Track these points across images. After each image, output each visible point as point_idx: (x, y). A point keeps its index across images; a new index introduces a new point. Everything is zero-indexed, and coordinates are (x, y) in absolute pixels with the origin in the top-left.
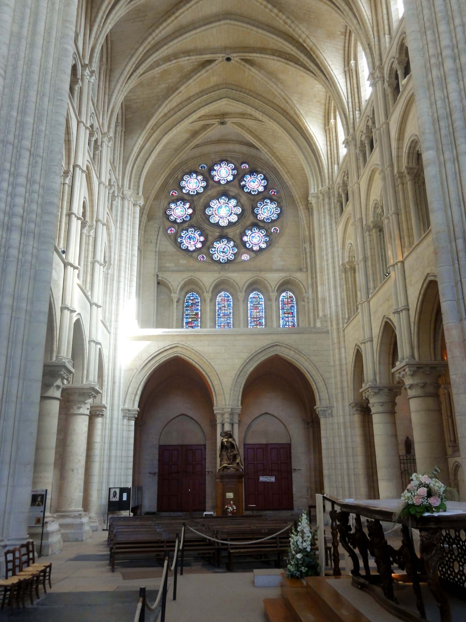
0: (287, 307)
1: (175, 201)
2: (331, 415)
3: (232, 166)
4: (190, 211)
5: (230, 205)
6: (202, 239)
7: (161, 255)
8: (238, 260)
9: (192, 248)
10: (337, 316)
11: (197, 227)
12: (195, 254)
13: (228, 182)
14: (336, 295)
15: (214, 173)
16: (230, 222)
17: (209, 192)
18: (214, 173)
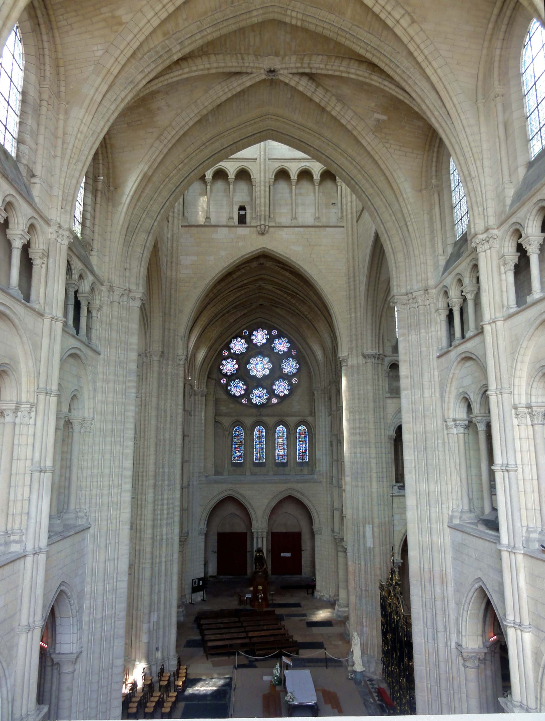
0: (302, 437)
1: (226, 358)
2: (321, 534)
3: (266, 331)
4: (237, 366)
5: (264, 362)
6: (245, 387)
7: (217, 401)
8: (269, 404)
9: (238, 394)
10: (326, 473)
12: (239, 399)
13: (263, 344)
14: (326, 460)
15: (253, 337)
16: (264, 375)
17: (250, 353)
18: (253, 337)
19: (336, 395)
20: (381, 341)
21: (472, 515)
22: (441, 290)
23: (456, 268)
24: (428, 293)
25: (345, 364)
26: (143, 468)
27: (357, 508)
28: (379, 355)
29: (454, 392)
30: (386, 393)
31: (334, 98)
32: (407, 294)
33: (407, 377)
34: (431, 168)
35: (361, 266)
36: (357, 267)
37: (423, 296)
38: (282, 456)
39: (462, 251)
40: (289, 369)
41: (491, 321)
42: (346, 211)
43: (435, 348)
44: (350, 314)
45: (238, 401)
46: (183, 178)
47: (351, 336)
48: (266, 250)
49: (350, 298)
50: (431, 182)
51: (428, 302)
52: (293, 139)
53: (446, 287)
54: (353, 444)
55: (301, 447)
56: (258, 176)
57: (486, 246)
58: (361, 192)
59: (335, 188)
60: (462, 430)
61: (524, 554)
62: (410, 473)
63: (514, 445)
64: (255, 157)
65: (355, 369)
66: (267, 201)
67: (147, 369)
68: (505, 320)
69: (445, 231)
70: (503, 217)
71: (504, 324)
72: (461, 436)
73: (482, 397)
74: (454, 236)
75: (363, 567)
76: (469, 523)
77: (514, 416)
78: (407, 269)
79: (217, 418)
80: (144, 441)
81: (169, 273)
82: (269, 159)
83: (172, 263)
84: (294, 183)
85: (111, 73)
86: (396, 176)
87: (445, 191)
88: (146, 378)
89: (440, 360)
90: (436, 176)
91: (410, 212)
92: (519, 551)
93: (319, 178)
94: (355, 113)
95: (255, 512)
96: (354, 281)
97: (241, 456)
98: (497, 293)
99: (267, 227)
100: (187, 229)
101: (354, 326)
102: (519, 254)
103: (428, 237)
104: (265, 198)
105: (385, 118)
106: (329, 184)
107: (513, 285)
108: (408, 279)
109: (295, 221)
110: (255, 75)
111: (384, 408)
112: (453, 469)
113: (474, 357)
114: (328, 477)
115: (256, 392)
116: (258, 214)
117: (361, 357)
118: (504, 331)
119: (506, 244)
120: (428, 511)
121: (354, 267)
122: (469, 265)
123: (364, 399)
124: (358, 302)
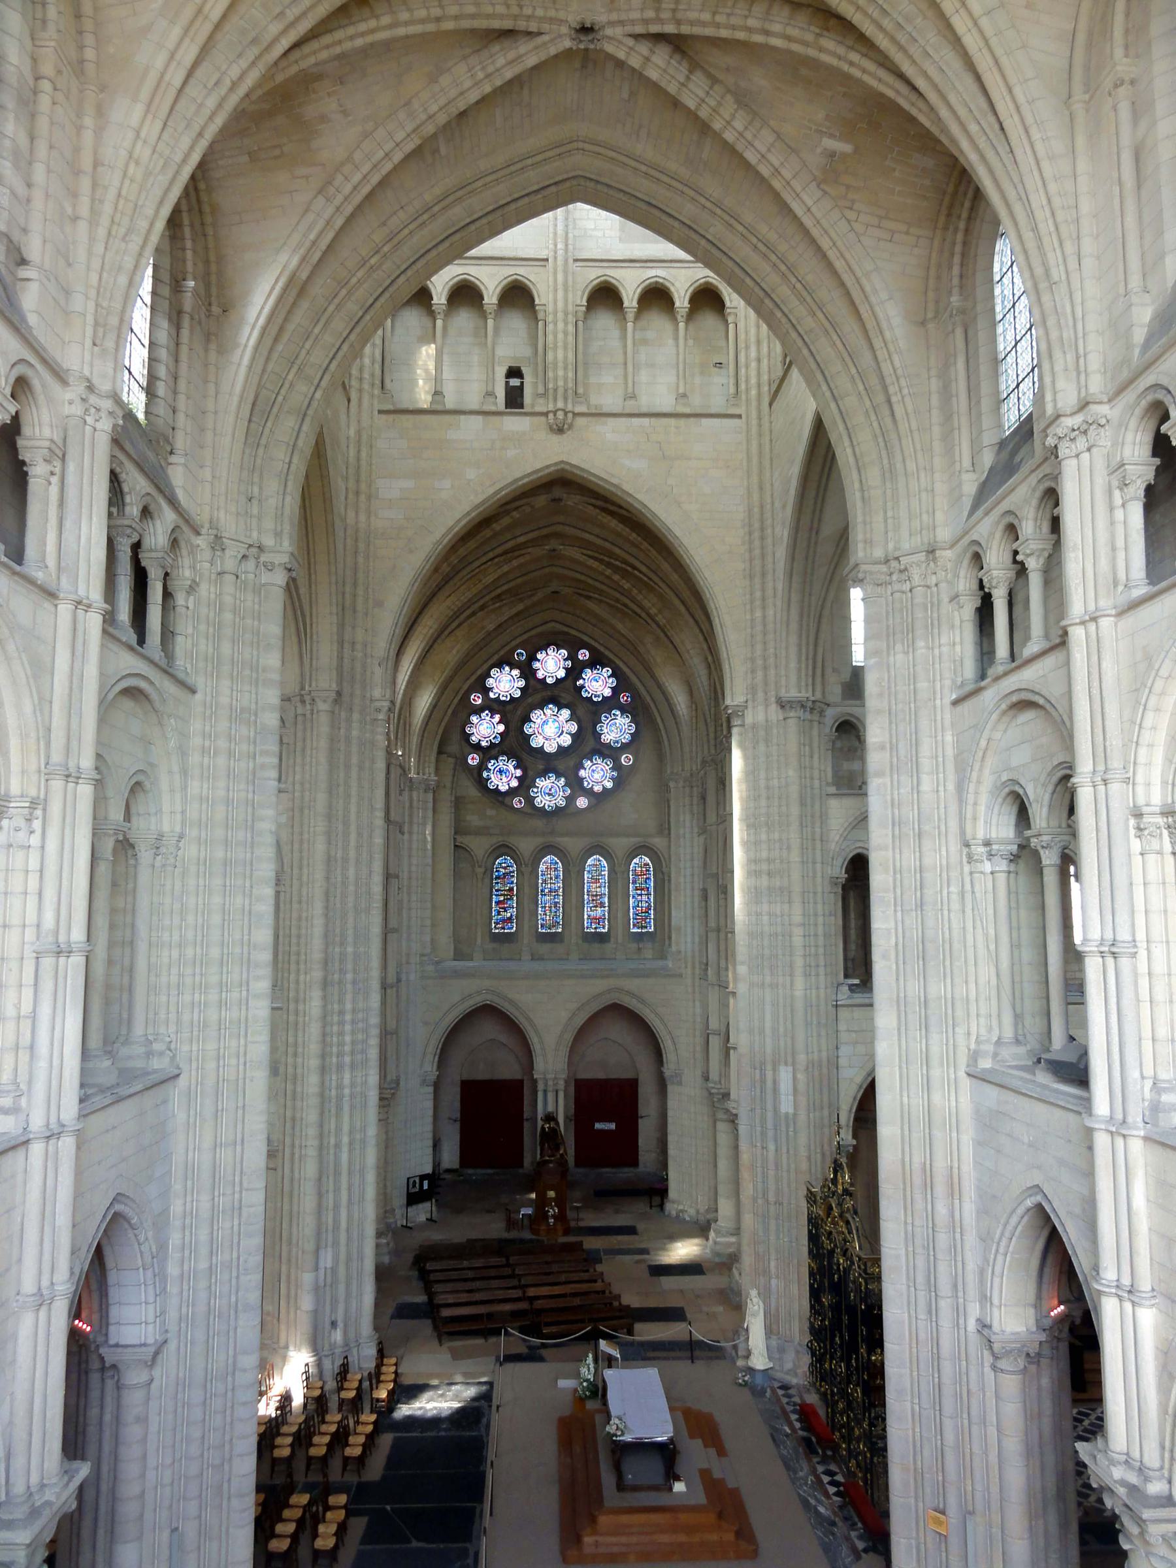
0: (641, 880)
1: (478, 711)
2: (680, 1083)
3: (564, 652)
4: (501, 728)
6: (519, 773)
7: (459, 803)
9: (503, 788)
10: (693, 957)
11: (511, 755)
12: (507, 800)
14: (693, 927)
15: (536, 665)
16: (559, 746)
17: (530, 700)
18: (536, 665)
19: (717, 790)
20: (819, 672)
21: (1021, 1050)
22: (965, 551)
23: (1004, 498)
24: (935, 560)
25: (739, 723)
26: (298, 944)
27: (762, 1031)
28: (814, 702)
29: (988, 780)
30: (828, 784)
31: (729, 98)
32: (887, 561)
33: (883, 748)
34: (950, 268)
35: (777, 504)
36: (769, 507)
37: (924, 565)
38: (598, 920)
39: (1018, 459)
40: (613, 735)
41: (1087, 618)
42: (747, 381)
43: (948, 683)
44: (752, 611)
45: (502, 803)
46: (381, 290)
47: (753, 660)
48: (567, 467)
49: (751, 577)
50: (950, 303)
51: (933, 580)
52: (633, 201)
53: (976, 543)
54: (754, 895)
55: (639, 901)
56: (551, 296)
57: (1081, 443)
58: (788, 326)
59: (721, 327)
60: (1003, 865)
61: (1146, 1139)
62: (885, 957)
63: (1132, 898)
64: (543, 255)
65: (762, 733)
66: (571, 356)
67: (305, 730)
68: (1120, 614)
69: (980, 415)
70: (1125, 374)
71: (1116, 624)
72: (1002, 878)
73: (1053, 793)
74: (1000, 426)
75: (771, 1155)
76: (1017, 1068)
77: (1132, 832)
78: (889, 504)
79: (460, 839)
80: (301, 885)
81: (351, 519)
82: (576, 260)
83: (357, 493)
84: (630, 316)
85: (206, 17)
86: (868, 288)
87: (981, 323)
88: (303, 750)
89: (959, 708)
90: (961, 287)
91: (899, 372)
92: (1135, 1133)
93: (686, 304)
94: (779, 136)
95: (540, 1037)
96: (762, 538)
97: (510, 919)
98: (1103, 551)
99: (570, 415)
100: (391, 417)
101: (759, 638)
102: (1157, 461)
103: (936, 430)
104: (565, 348)
105: (847, 148)
106: (708, 320)
107: (1142, 532)
108: (890, 527)
109: (632, 402)
110: (546, 38)
111: (824, 817)
112: (982, 951)
113: (1041, 701)
114: (697, 966)
115: (543, 783)
116: (551, 386)
117: (774, 707)
118: (1117, 640)
119: (1130, 437)
120: (924, 1041)
121: (762, 507)
122: (1034, 490)
123: (780, 798)
124: (770, 585)
